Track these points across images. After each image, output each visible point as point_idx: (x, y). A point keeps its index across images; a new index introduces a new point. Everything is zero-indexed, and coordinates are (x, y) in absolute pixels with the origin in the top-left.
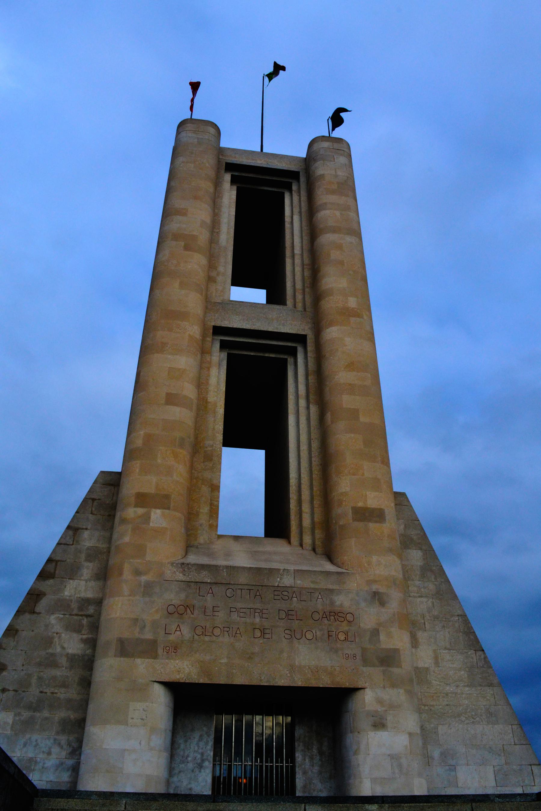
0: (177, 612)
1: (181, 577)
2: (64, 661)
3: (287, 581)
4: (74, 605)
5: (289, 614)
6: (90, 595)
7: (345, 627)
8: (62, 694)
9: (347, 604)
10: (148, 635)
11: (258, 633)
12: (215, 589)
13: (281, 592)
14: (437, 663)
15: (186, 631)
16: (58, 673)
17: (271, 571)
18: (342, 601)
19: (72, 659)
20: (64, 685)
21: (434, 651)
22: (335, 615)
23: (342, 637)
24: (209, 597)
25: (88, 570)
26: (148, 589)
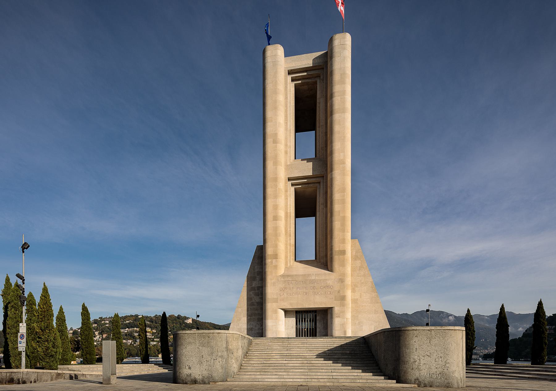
0: (282, 290)
1: (282, 279)
2: (256, 304)
3: (313, 278)
4: (256, 289)
5: (314, 288)
6: (260, 285)
7: (330, 290)
8: (257, 312)
10: (276, 297)
13: (312, 282)
14: (361, 297)
15: (285, 294)
16: (254, 307)
17: (309, 275)
19: (258, 303)
20: (257, 310)
21: (361, 294)
22: (327, 286)
23: (329, 293)
24: (291, 285)
25: (258, 278)
26: (274, 284)
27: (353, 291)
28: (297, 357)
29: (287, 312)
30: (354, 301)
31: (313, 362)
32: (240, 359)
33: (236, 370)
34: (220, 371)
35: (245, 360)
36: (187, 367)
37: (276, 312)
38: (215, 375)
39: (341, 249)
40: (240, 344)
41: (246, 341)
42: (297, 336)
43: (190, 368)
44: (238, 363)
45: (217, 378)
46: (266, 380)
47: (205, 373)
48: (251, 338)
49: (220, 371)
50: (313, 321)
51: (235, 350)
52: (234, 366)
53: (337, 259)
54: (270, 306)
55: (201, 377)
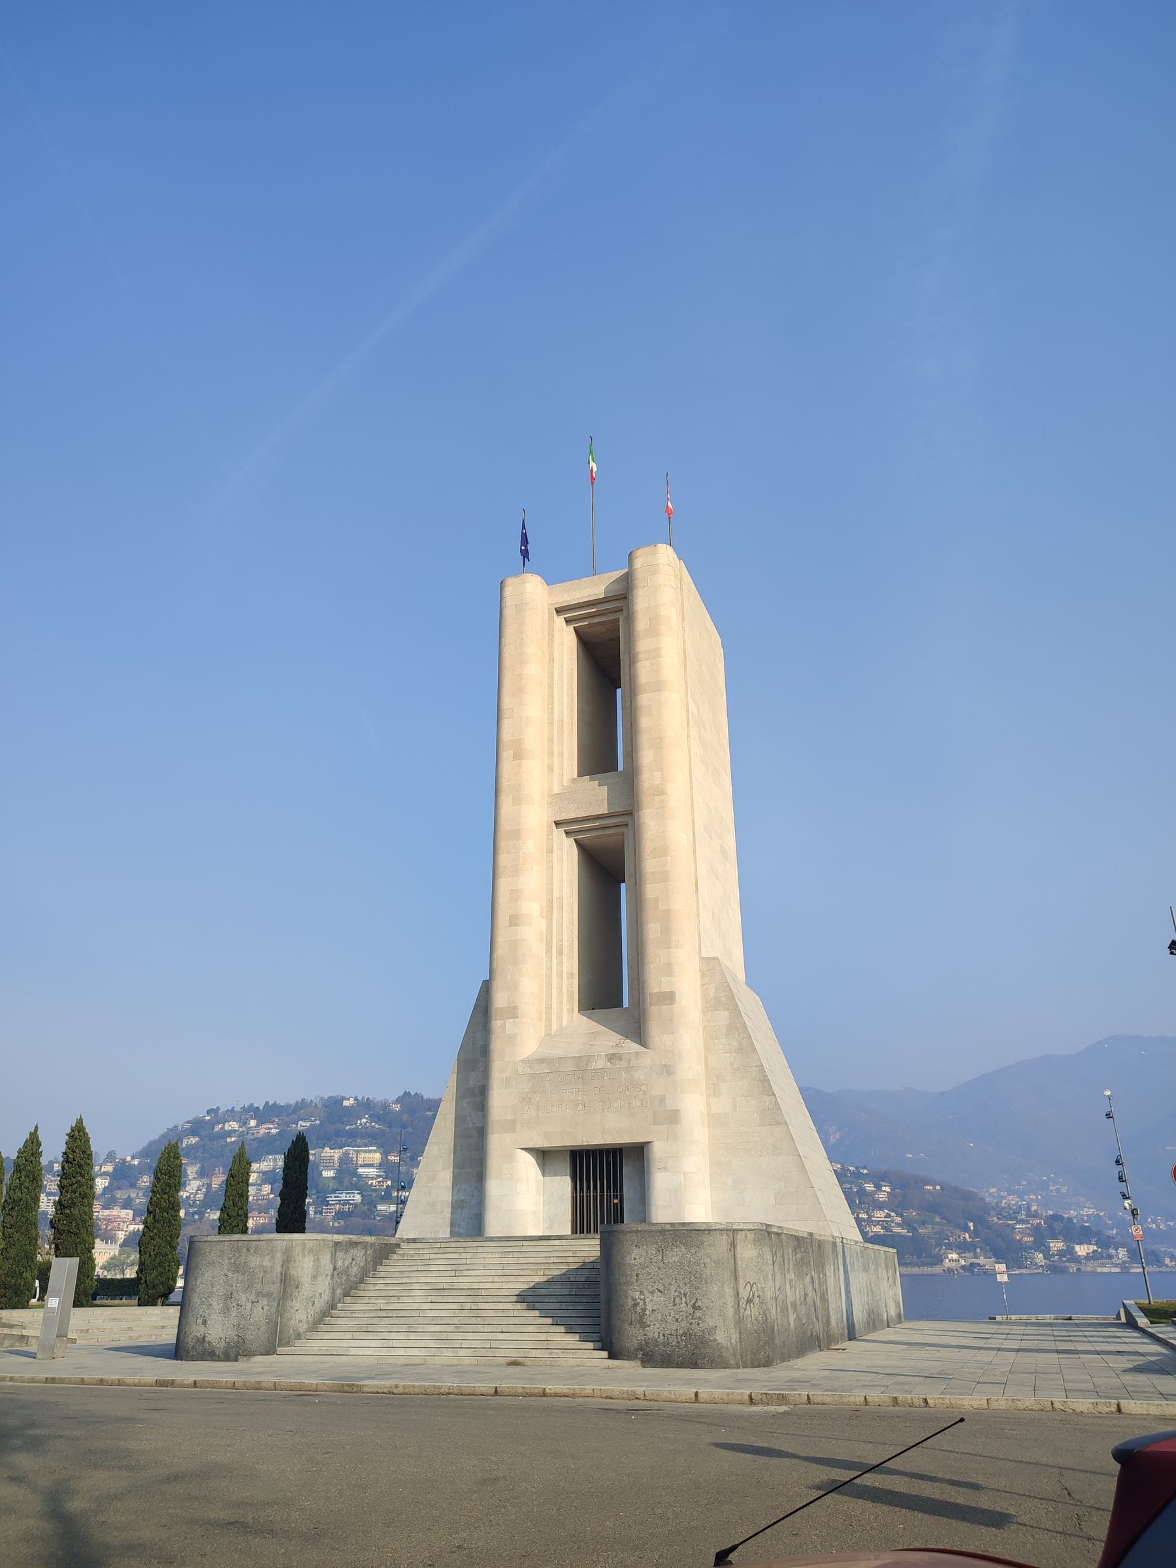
9: (642, 1078)
11: (580, 1107)
14: (735, 1109)
17: (589, 1058)
18: (639, 1075)
27: (713, 1090)
29: (544, 1156)
30: (715, 1120)
31: (482, 1306)
33: (303, 1327)
35: (348, 1299)
36: (200, 1321)
37: (510, 1158)
39: (665, 988)
43: (204, 1322)
46: (353, 1352)
47: (232, 1334)
53: (655, 1014)
54: (497, 1142)
55: (222, 1345)
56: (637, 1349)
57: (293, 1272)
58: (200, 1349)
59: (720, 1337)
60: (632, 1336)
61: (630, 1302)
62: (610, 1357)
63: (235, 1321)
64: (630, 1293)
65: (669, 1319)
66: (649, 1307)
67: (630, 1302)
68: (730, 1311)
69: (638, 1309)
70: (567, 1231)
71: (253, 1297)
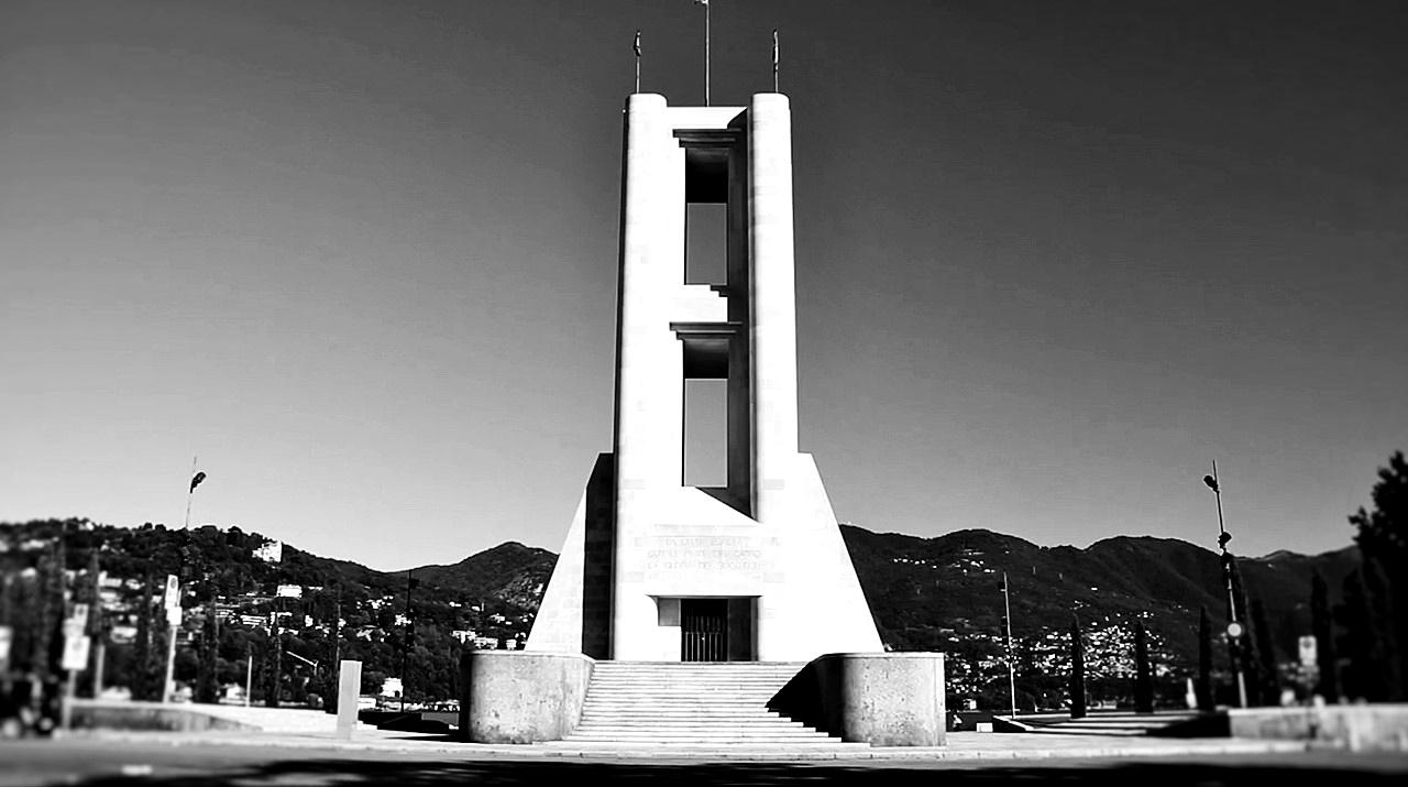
12: (676, 539)
28: (687, 700)
29: (661, 602)
32: (581, 701)
33: (575, 723)
34: (551, 722)
36: (493, 714)
38: (541, 728)
40: (582, 676)
41: (588, 669)
42: (683, 659)
43: (497, 715)
44: (579, 709)
45: (545, 734)
47: (525, 726)
48: (594, 661)
49: (551, 722)
50: (717, 628)
51: (575, 687)
52: (573, 716)
56: (867, 736)
57: (568, 681)
58: (495, 735)
59: (925, 726)
60: (863, 728)
61: (863, 705)
62: (843, 741)
63: (528, 716)
64: (863, 699)
65: (892, 716)
66: (877, 708)
67: (863, 705)
68: (933, 709)
69: (869, 710)
70: (679, 659)
71: (541, 698)
